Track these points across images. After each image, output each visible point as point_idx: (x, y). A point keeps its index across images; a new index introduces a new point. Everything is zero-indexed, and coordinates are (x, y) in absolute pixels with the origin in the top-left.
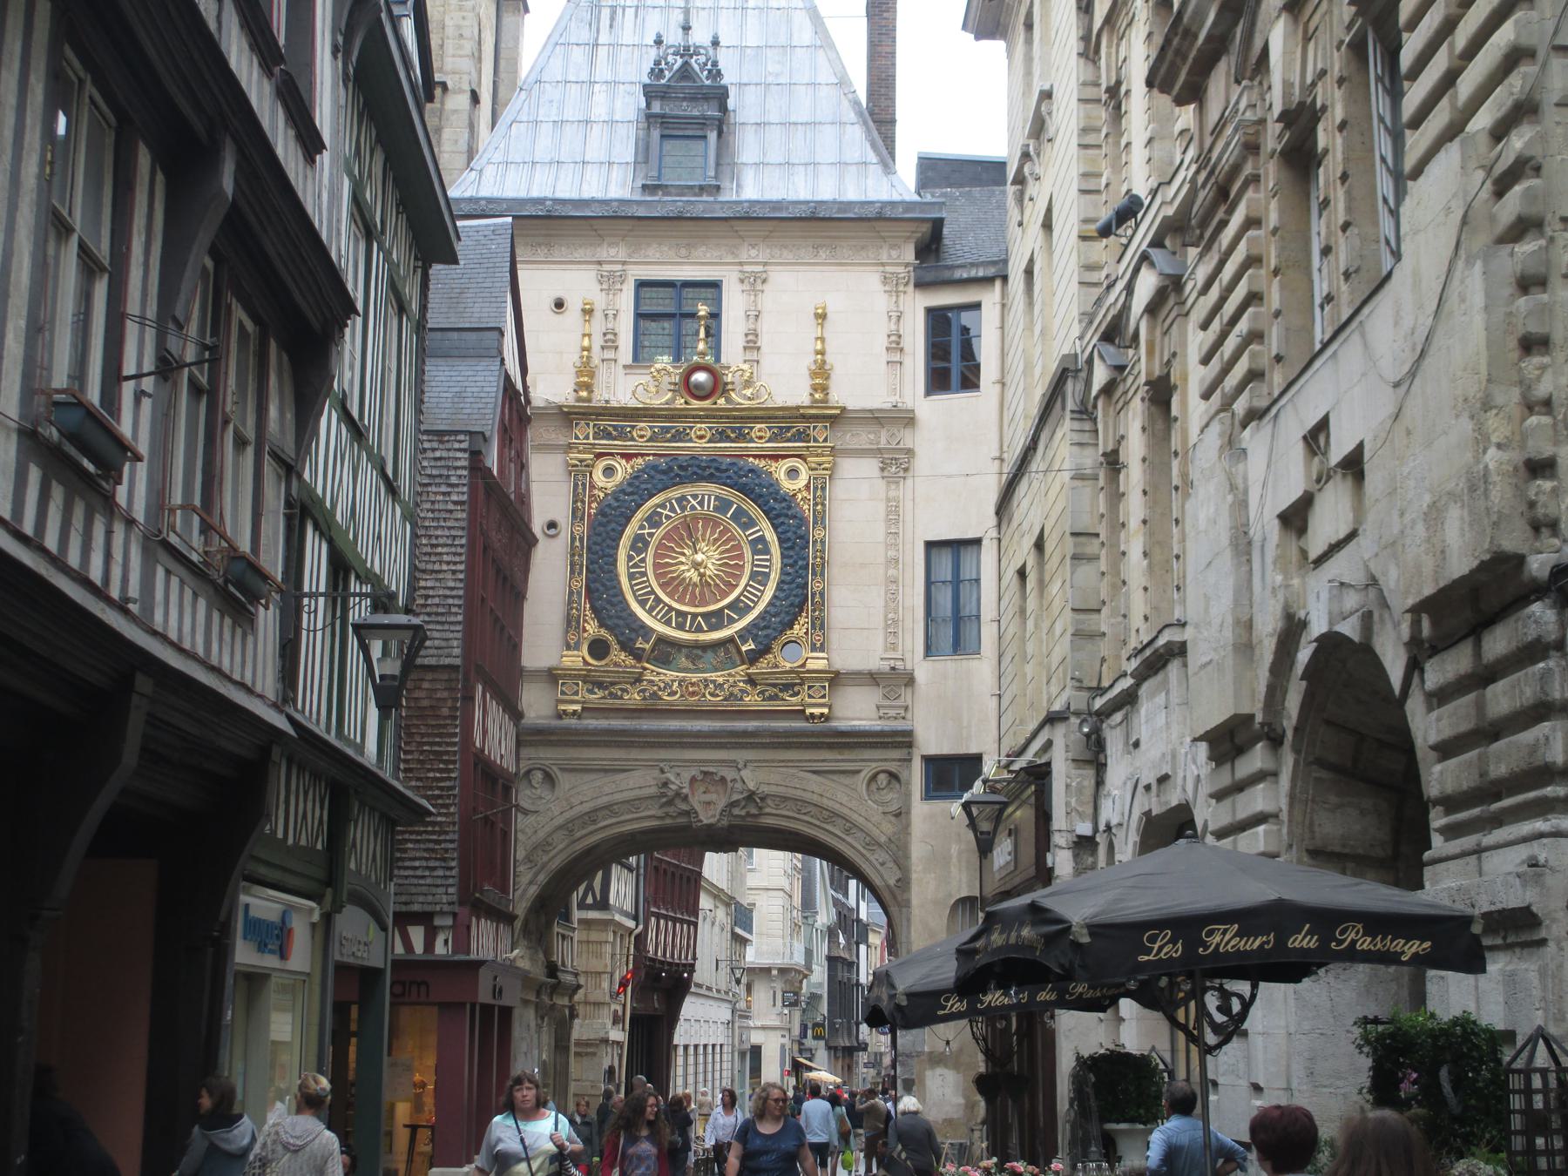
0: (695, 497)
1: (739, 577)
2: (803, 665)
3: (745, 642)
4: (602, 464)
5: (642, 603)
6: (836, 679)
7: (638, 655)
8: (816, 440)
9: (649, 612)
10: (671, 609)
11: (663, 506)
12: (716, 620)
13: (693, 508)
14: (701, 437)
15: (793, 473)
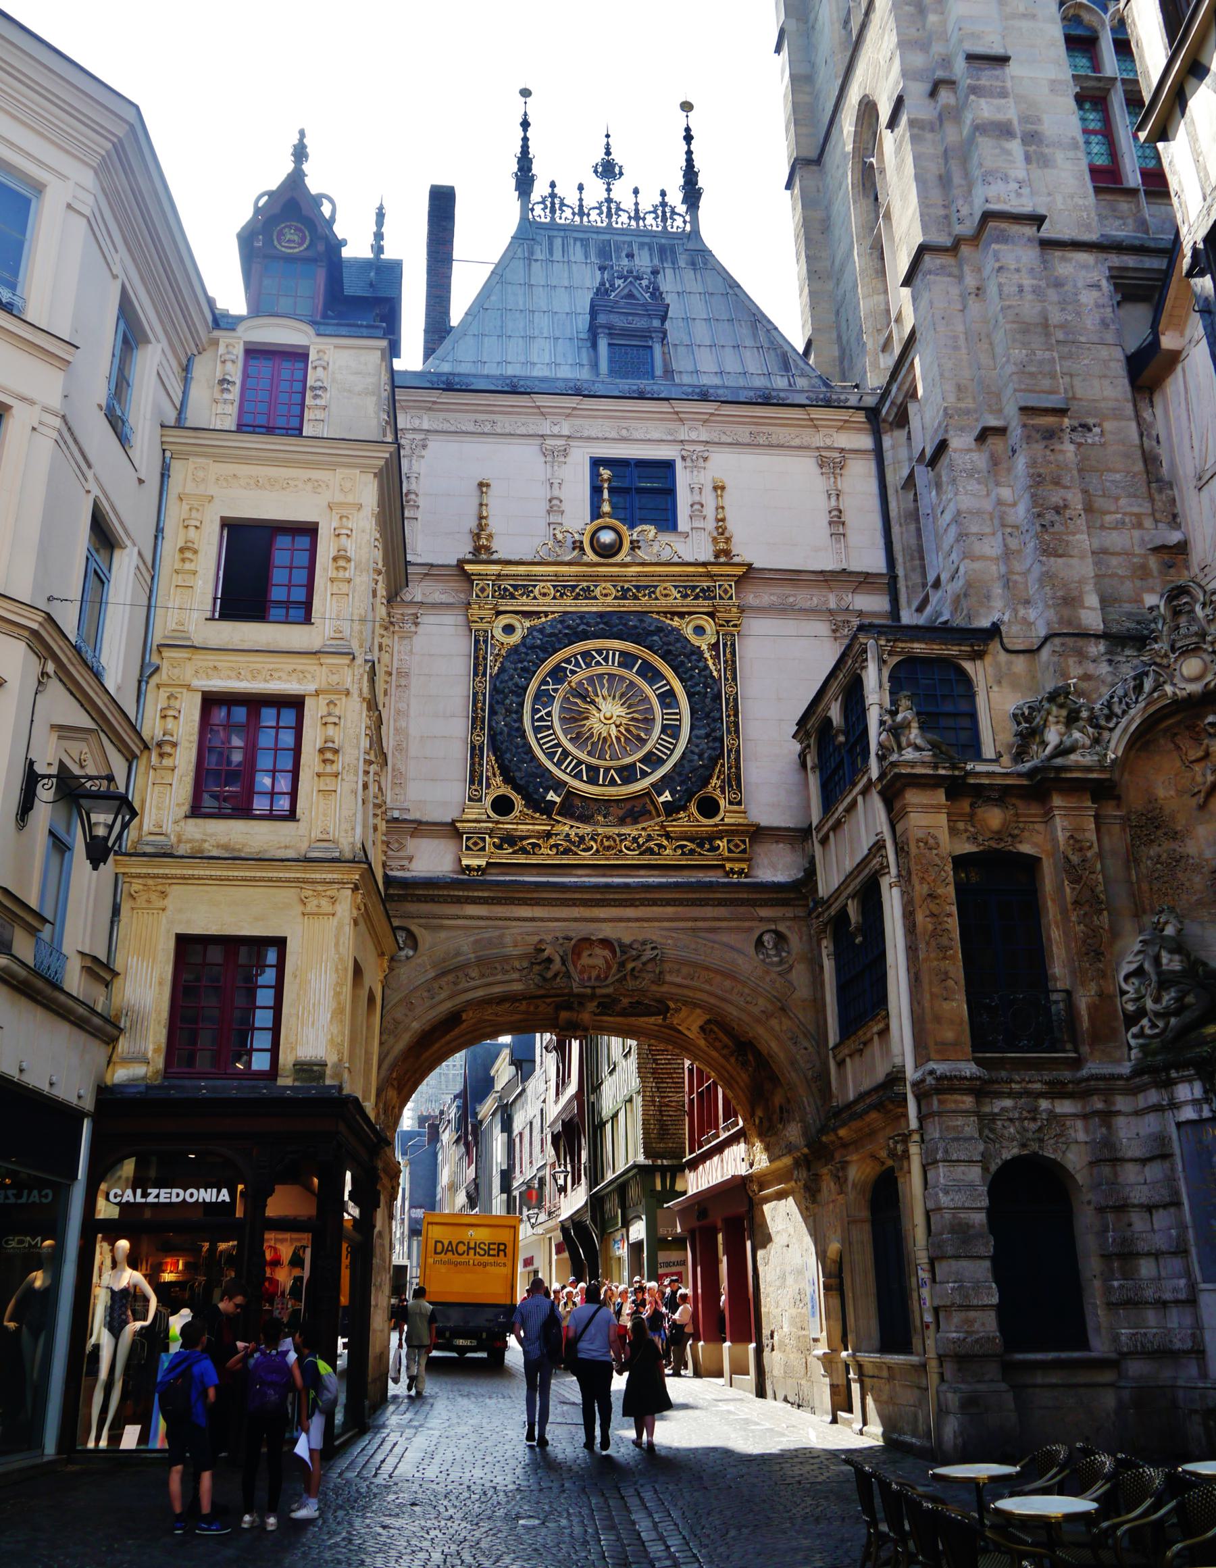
0: (599, 652)
1: (648, 732)
2: (722, 820)
3: (660, 795)
4: (503, 620)
5: (550, 756)
6: (758, 833)
7: (546, 809)
8: (721, 598)
9: (558, 765)
10: (580, 763)
11: (568, 661)
12: (628, 774)
13: (598, 663)
14: (606, 595)
15: (700, 630)
